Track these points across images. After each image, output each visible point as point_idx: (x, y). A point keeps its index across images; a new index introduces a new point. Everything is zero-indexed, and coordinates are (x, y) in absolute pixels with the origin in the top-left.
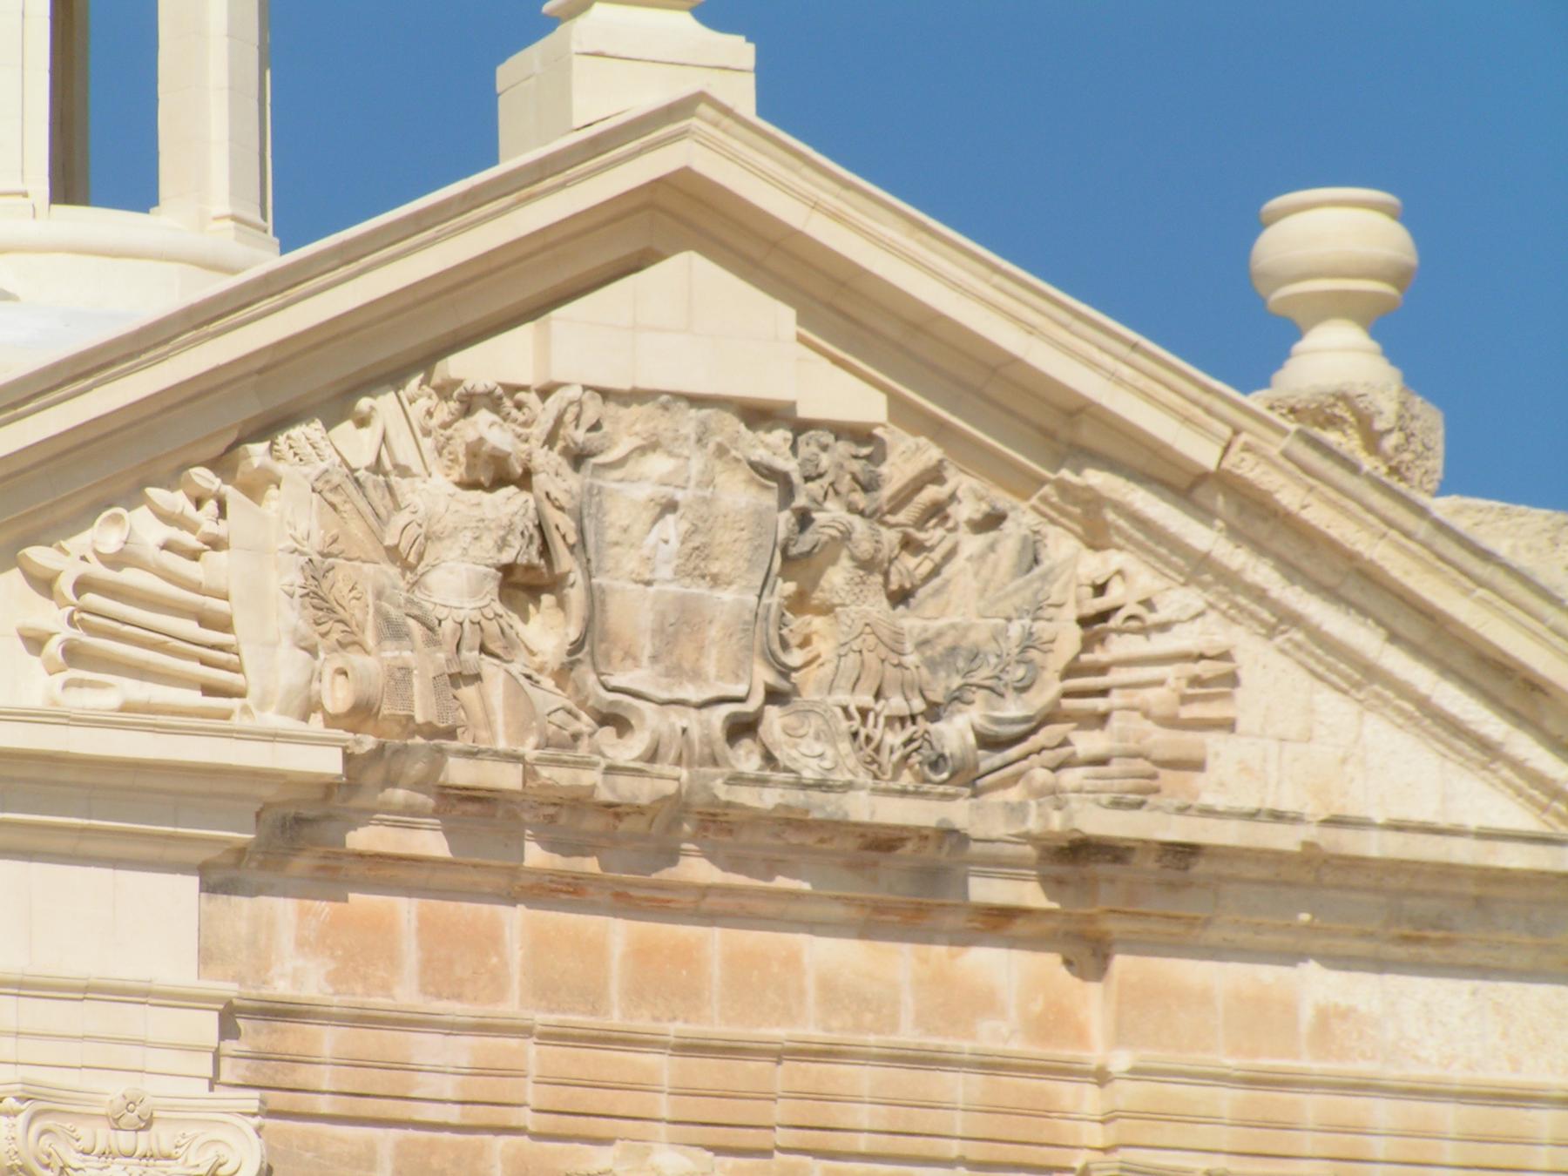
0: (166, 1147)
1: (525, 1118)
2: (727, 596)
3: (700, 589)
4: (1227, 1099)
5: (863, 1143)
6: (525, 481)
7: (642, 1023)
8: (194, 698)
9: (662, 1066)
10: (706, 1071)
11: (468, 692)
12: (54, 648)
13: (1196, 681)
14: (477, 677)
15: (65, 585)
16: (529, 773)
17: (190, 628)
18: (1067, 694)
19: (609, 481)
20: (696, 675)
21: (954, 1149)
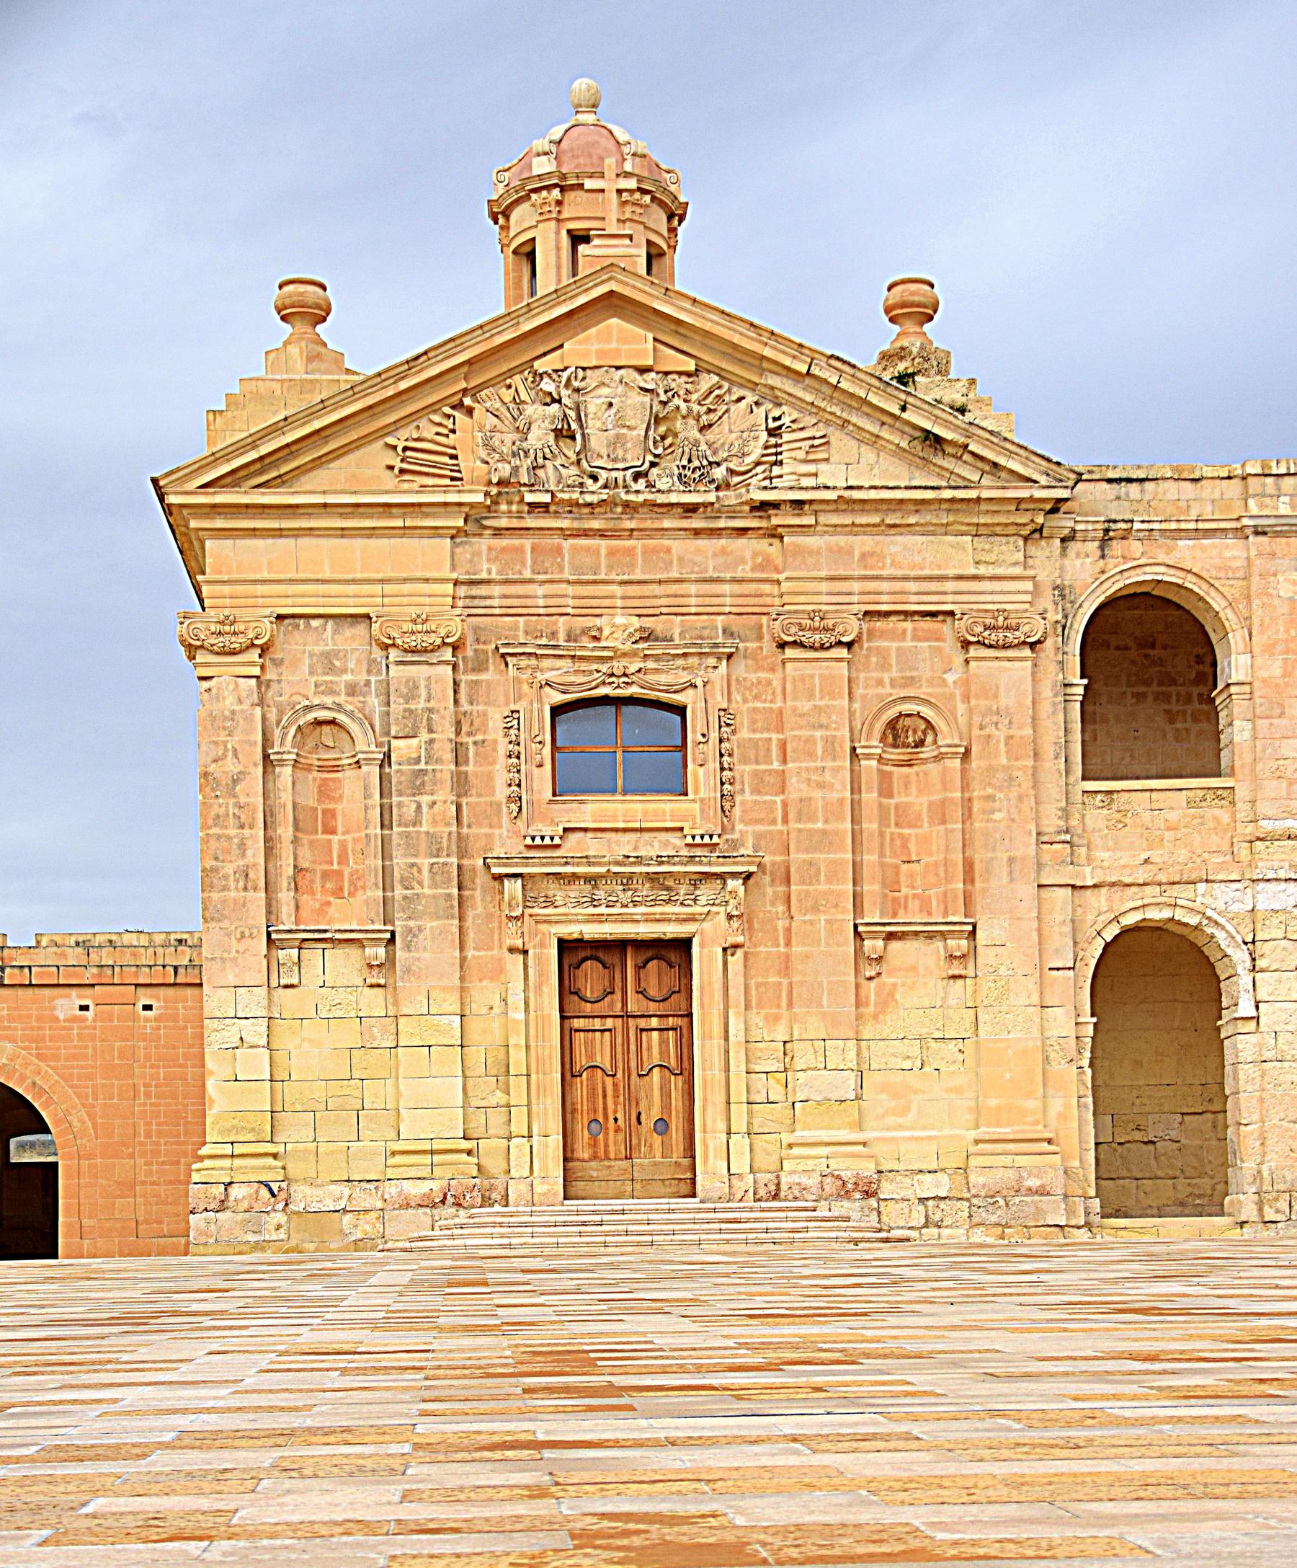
0: (433, 628)
1: (570, 610)
2: (635, 433)
3: (624, 431)
4: (824, 586)
5: (693, 610)
6: (559, 401)
7: (613, 576)
8: (447, 482)
9: (618, 590)
10: (633, 590)
11: (541, 473)
12: (396, 471)
13: (813, 446)
14: (543, 467)
15: (399, 450)
16: (553, 495)
17: (446, 460)
18: (763, 456)
19: (587, 398)
20: (625, 460)
21: (727, 609)
